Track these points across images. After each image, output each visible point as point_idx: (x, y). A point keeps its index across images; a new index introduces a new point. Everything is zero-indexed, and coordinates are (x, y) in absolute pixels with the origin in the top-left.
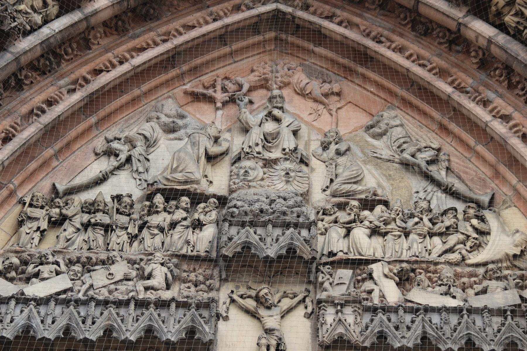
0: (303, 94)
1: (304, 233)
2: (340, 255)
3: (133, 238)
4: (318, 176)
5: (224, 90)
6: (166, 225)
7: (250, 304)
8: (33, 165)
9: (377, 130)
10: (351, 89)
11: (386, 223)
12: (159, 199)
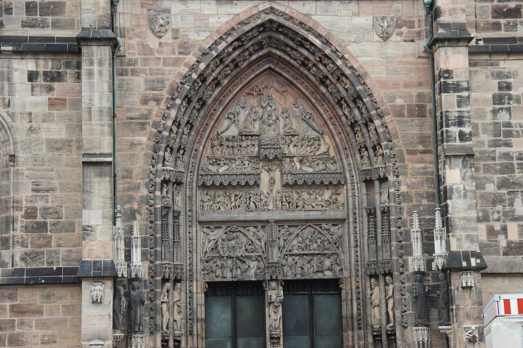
1: (279, 150)
2: (287, 155)
3: (238, 150)
4: (281, 123)
5: (256, 92)
6: (246, 146)
10: (289, 90)
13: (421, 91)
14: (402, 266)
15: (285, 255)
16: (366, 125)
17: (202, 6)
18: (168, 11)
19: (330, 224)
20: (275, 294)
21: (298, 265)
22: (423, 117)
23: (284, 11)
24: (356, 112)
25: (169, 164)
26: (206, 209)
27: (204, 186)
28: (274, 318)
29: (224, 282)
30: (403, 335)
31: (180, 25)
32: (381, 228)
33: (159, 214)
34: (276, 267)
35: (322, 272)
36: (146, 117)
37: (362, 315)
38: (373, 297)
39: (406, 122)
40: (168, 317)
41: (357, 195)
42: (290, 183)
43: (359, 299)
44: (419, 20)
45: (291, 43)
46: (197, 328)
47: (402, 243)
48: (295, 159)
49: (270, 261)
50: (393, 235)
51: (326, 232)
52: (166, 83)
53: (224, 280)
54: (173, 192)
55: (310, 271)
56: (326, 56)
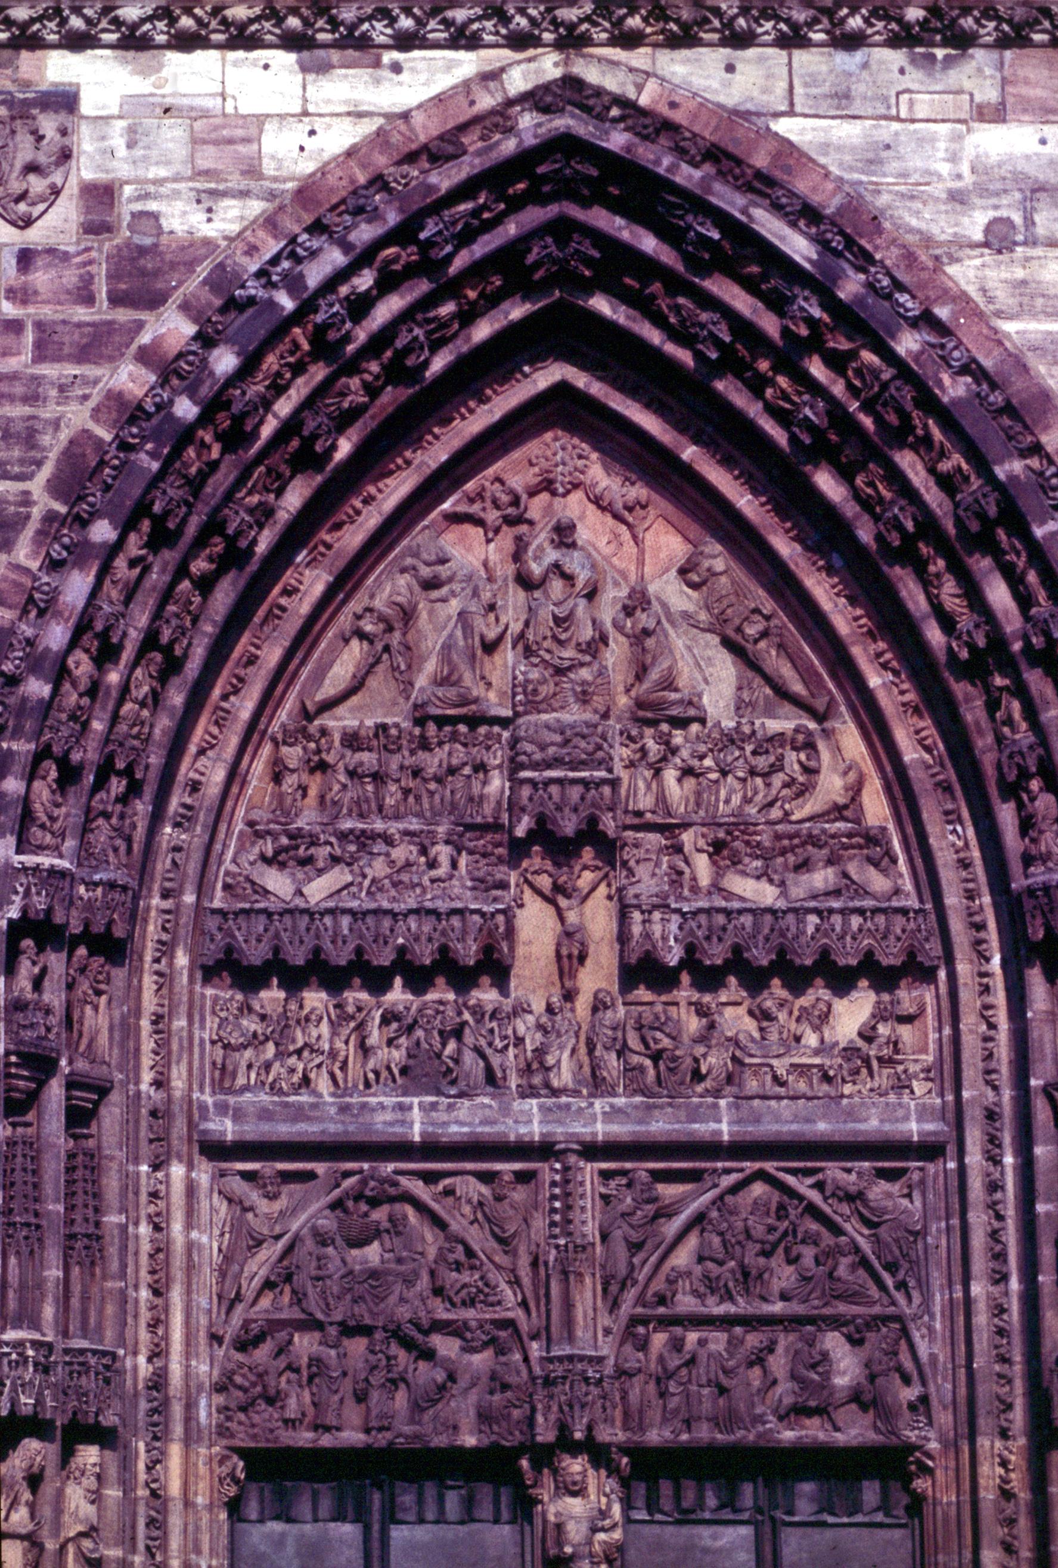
0: (597, 501)
3: (406, 792)
11: (702, 758)
12: (432, 728)
29: (325, 1450)
31: (122, 169)
52: (46, 440)
53: (326, 1441)
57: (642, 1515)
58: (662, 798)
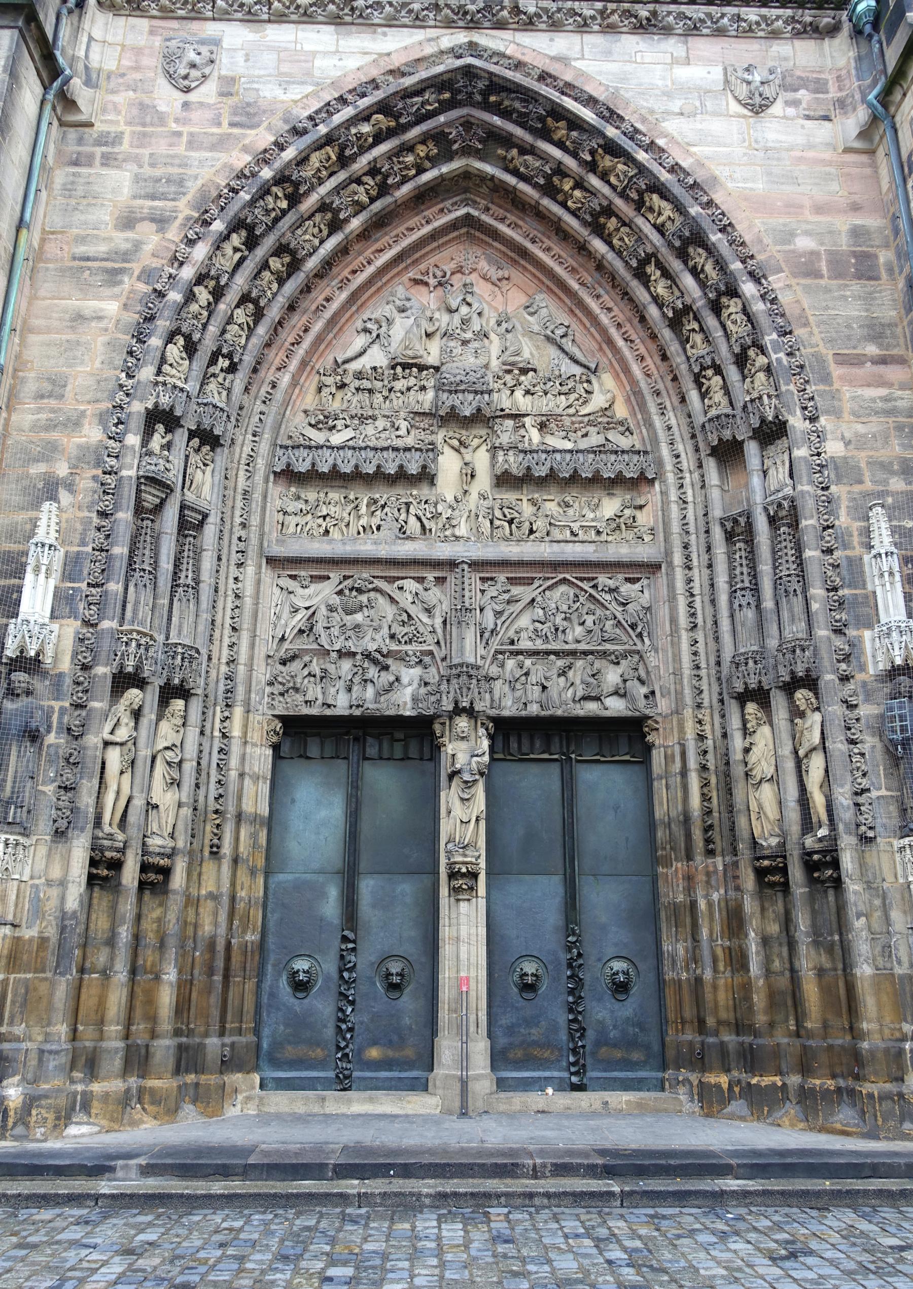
0: (485, 278)
1: (486, 396)
3: (386, 398)
4: (495, 345)
7: (456, 443)
8: (322, 347)
9: (531, 310)
10: (516, 275)
12: (399, 369)
13: (859, 222)
14: (847, 658)
15: (498, 652)
16: (716, 308)
17: (300, 34)
18: (217, 42)
19: (621, 577)
20: (465, 748)
21: (533, 679)
22: (870, 278)
23: (502, 49)
24: (688, 281)
25: (174, 372)
26: (292, 529)
27: (289, 475)
28: (462, 816)
30: (862, 864)
32: (770, 562)
33: (128, 495)
34: (470, 676)
35: (597, 699)
36: (126, 256)
37: (716, 814)
38: (752, 758)
39: (827, 290)
40: (126, 791)
41: (690, 499)
42: (515, 471)
43: (704, 768)
44: (838, 77)
45: (518, 132)
46: (237, 839)
47: (840, 593)
48: (528, 421)
49: (456, 661)
50: (814, 572)
51: (608, 597)
52: (189, 184)
53: (328, 712)
54: (187, 457)
55: (564, 696)
56: (612, 149)
57: (501, 756)
58: (514, 403)
